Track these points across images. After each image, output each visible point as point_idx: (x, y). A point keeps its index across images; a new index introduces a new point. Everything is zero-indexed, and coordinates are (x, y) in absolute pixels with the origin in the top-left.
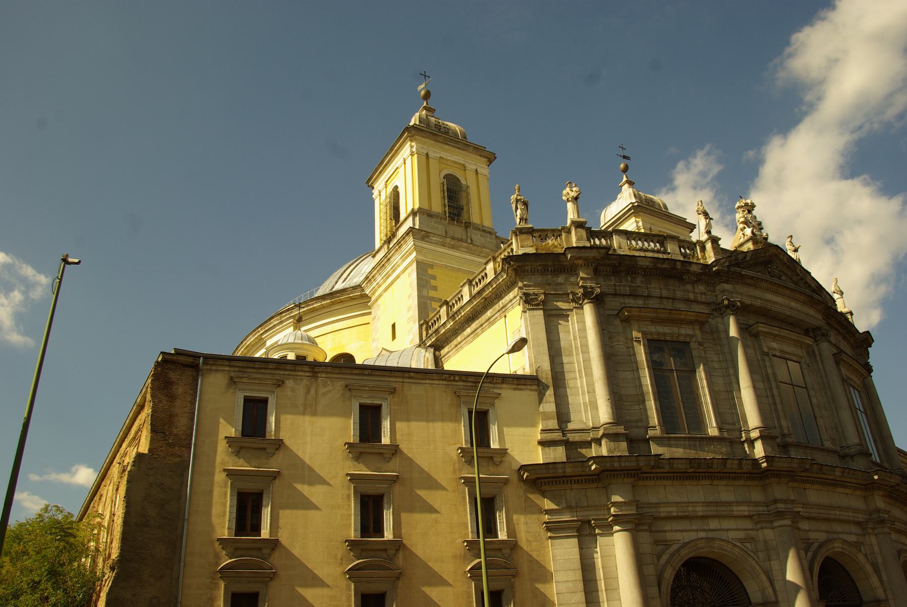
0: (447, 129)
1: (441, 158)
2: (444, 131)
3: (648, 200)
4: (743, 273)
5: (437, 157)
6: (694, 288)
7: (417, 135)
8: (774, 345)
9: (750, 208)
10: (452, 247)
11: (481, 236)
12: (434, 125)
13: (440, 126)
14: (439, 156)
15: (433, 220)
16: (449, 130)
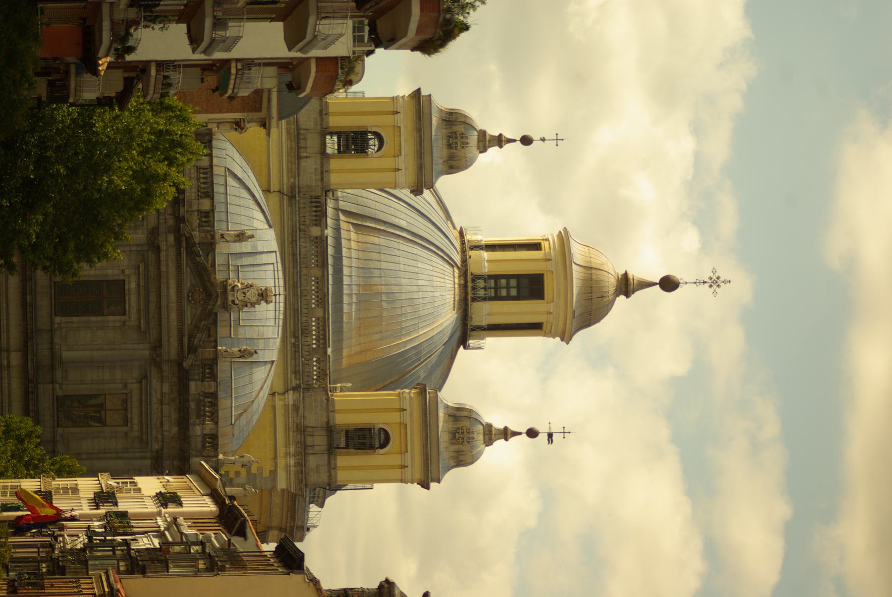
0: (456, 147)
1: (400, 127)
2: (451, 142)
3: (463, 433)
4: (182, 249)
5: (397, 123)
6: (170, 215)
7: (416, 101)
8: (133, 285)
9: (264, 295)
10: (289, 133)
11: (316, 168)
12: (455, 130)
13: (456, 138)
14: (399, 125)
15: (318, 116)
16: (456, 149)
